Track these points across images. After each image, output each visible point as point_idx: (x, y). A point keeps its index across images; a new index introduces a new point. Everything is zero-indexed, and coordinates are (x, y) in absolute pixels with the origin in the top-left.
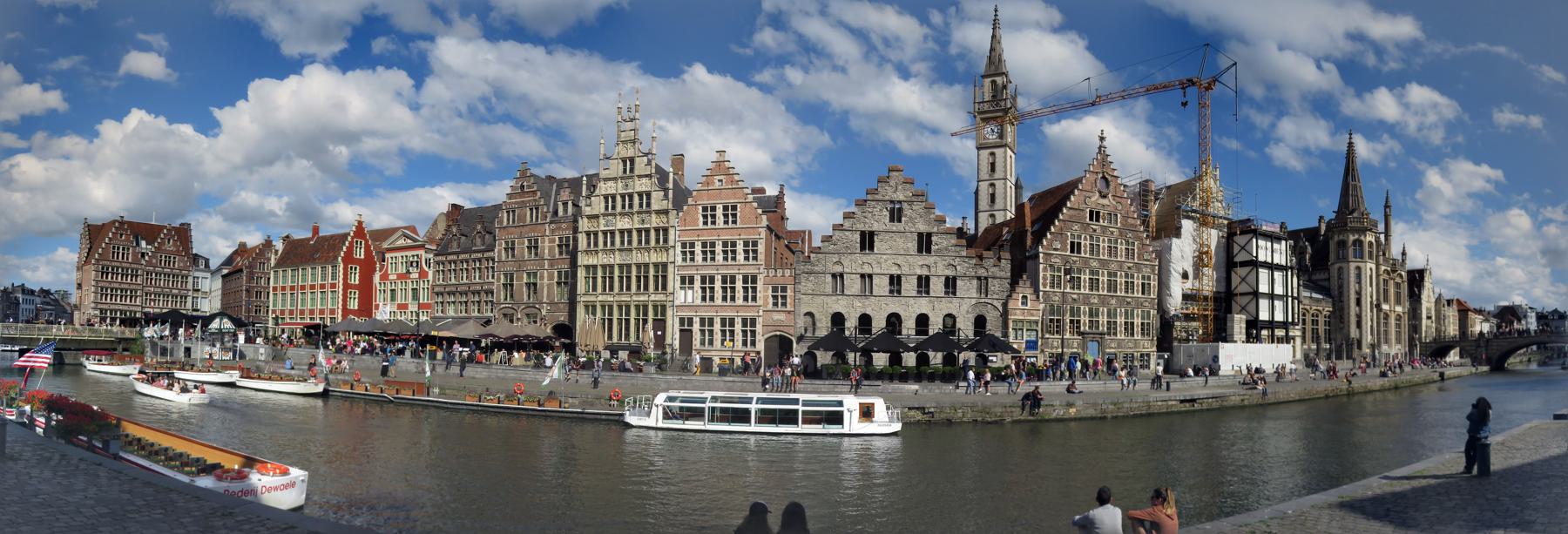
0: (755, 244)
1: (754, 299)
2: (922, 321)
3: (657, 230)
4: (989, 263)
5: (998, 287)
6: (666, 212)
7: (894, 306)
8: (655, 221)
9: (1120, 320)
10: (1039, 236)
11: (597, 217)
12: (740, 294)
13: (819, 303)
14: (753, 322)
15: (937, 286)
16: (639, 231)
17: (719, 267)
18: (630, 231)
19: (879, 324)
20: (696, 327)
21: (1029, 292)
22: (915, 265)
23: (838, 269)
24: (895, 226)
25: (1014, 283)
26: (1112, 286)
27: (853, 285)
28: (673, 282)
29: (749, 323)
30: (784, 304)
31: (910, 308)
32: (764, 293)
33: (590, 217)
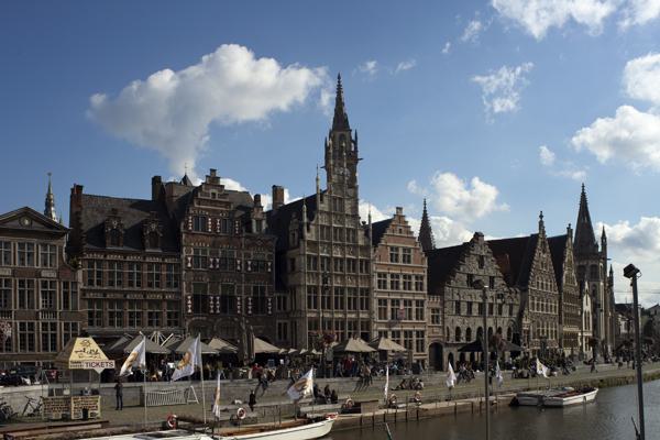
0: (422, 278)
1: (422, 319)
3: (361, 261)
4: (513, 295)
6: (365, 249)
11: (313, 245)
12: (414, 314)
14: (423, 332)
16: (349, 260)
18: (342, 260)
23: (457, 298)
27: (464, 307)
28: (375, 305)
29: (421, 334)
30: (438, 322)
32: (428, 314)
33: (309, 243)
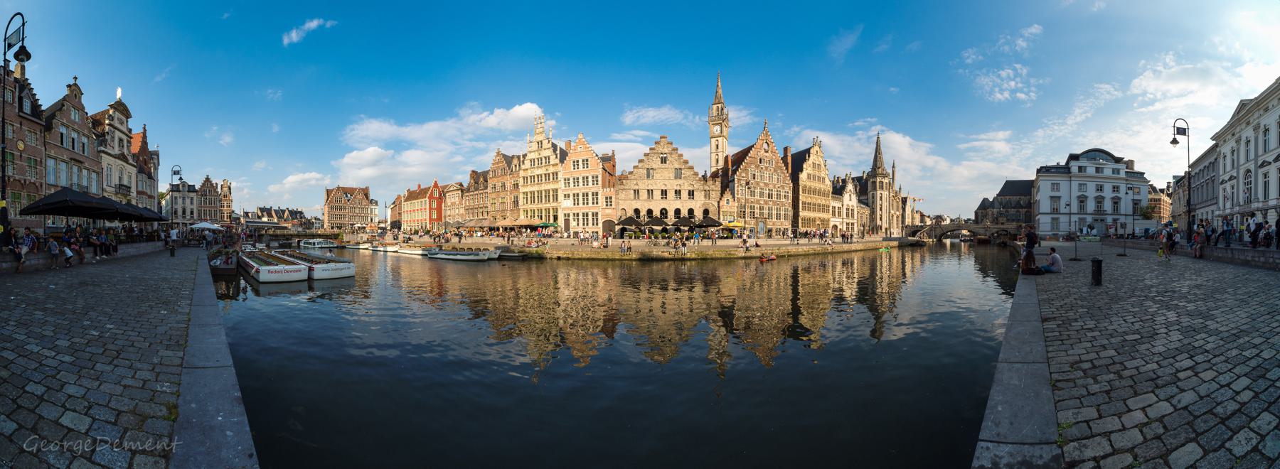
2: (678, 212)
5: (715, 195)
7: (664, 204)
8: (551, 170)
9: (774, 212)
10: (734, 172)
13: (626, 205)
15: (685, 195)
17: (581, 189)
19: (657, 213)
20: (571, 218)
21: (730, 197)
22: (672, 185)
24: (664, 166)
25: (722, 193)
26: (770, 196)
27: (644, 195)
28: (561, 197)
31: (671, 205)
32: (601, 200)
